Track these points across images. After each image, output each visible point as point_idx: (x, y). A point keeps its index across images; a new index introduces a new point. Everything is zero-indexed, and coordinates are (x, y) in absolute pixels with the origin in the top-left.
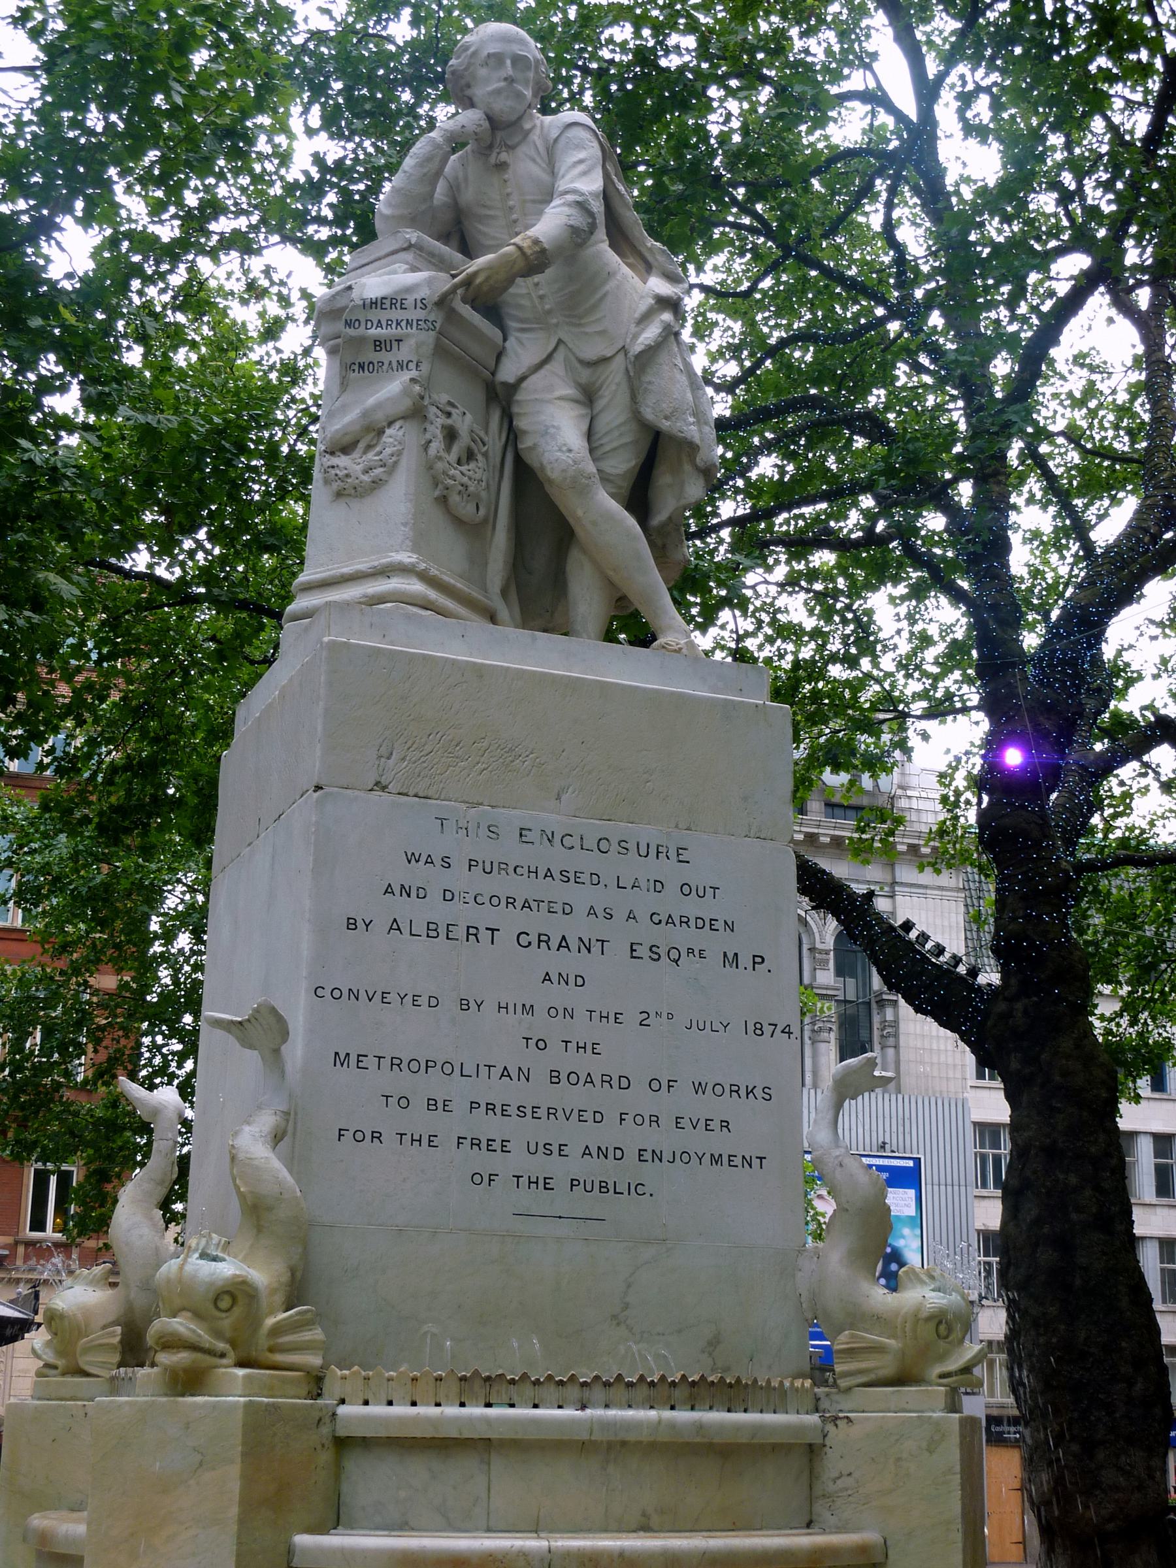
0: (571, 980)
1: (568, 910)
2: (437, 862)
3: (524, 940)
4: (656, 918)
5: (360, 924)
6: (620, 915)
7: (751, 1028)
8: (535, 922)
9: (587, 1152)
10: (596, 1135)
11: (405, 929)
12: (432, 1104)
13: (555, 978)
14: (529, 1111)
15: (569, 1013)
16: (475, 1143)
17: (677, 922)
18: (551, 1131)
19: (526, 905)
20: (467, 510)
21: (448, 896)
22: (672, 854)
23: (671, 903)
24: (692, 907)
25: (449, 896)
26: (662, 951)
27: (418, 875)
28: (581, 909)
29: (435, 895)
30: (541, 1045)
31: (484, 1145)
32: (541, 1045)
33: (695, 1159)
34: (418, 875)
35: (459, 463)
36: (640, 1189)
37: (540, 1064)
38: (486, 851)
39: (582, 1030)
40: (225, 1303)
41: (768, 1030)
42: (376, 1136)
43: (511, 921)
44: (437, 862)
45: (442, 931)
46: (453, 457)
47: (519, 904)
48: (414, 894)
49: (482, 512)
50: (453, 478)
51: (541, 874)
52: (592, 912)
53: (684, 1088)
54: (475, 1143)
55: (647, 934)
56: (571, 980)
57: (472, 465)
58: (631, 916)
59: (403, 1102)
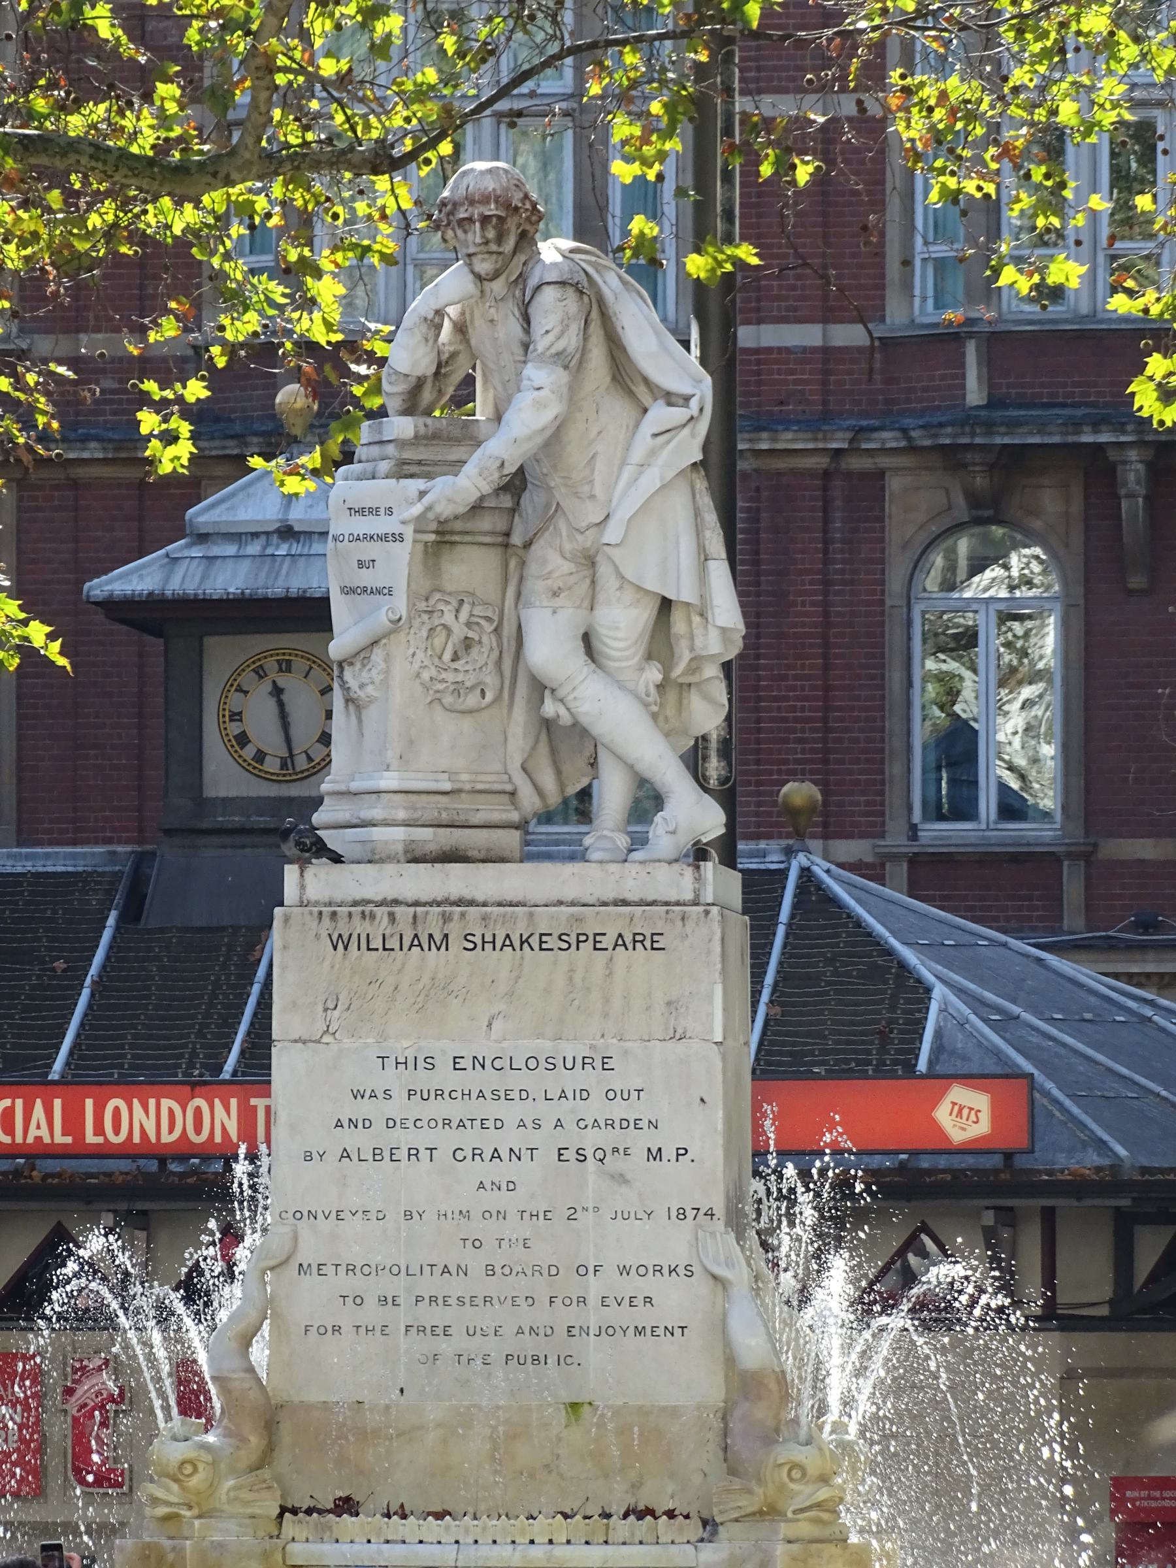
0: (504, 1187)
1: (499, 1124)
2: (380, 1095)
3: (459, 1155)
4: (582, 1124)
5: (315, 1155)
6: (548, 1125)
7: (674, 1213)
8: (470, 1138)
9: (520, 1331)
10: (527, 1316)
11: (354, 1157)
12: (383, 1301)
13: (488, 1186)
14: (467, 1300)
15: (501, 1215)
16: (422, 1330)
17: (603, 1125)
18: (485, 1318)
19: (461, 1124)
20: (472, 700)
21: (391, 1124)
22: (598, 1064)
23: (596, 1108)
24: (618, 1110)
25: (391, 1124)
26: (589, 1153)
27: (365, 1108)
28: (511, 1123)
29: (379, 1125)
30: (477, 1244)
31: (428, 1331)
32: (477, 1244)
33: (619, 1332)
34: (365, 1108)
35: (455, 658)
36: (569, 1360)
37: (475, 1261)
38: (423, 1080)
39: (514, 1228)
40: (188, 1469)
41: (690, 1214)
42: (337, 1329)
43: (447, 1140)
44: (380, 1095)
45: (387, 1154)
46: (447, 656)
47: (454, 1124)
48: (360, 1125)
49: (489, 696)
50: (443, 681)
51: (474, 1095)
52: (522, 1124)
53: (610, 1273)
54: (422, 1330)
55: (571, 1137)
56: (504, 1187)
57: (475, 651)
58: (559, 1124)
59: (358, 1301)
